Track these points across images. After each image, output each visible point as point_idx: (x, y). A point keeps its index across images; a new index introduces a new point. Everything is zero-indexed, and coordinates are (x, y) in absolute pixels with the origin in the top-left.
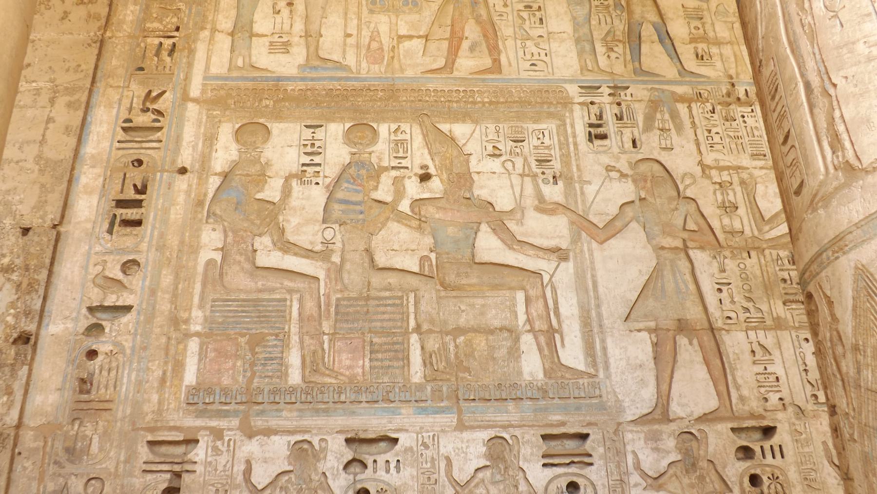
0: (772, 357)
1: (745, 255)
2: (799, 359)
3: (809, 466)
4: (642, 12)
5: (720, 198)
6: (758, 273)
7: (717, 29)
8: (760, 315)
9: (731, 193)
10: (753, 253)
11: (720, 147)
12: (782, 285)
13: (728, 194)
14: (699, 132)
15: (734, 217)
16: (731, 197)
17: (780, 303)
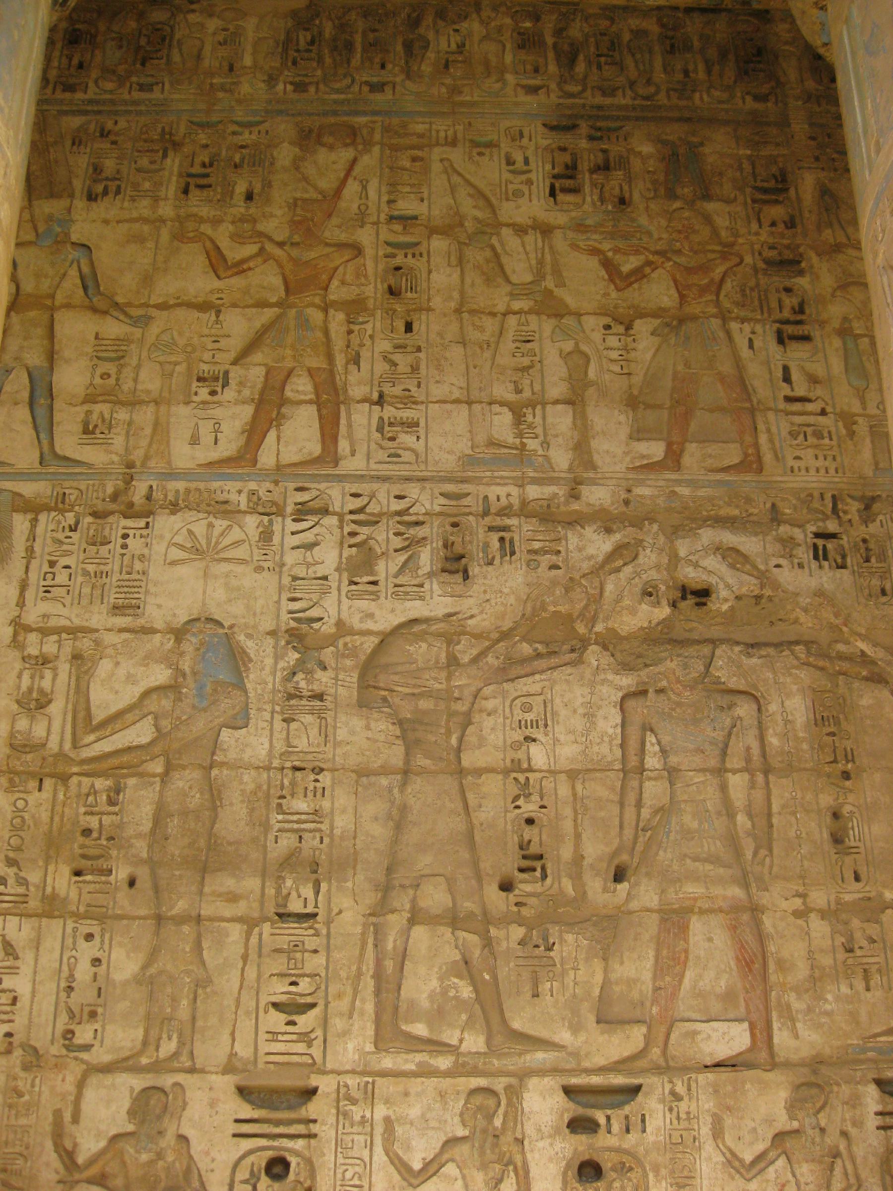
0: (18, 963)
1: (33, 784)
2: (65, 968)
3: (17, 1149)
4: (22, 348)
5: (26, 681)
6: (45, 816)
7: (143, 375)
8: (21, 890)
9: (48, 674)
10: (48, 783)
11: (62, 591)
12: (81, 839)
13: (42, 677)
14: (34, 564)
15: (39, 717)
16: (46, 684)
17: (65, 871)
